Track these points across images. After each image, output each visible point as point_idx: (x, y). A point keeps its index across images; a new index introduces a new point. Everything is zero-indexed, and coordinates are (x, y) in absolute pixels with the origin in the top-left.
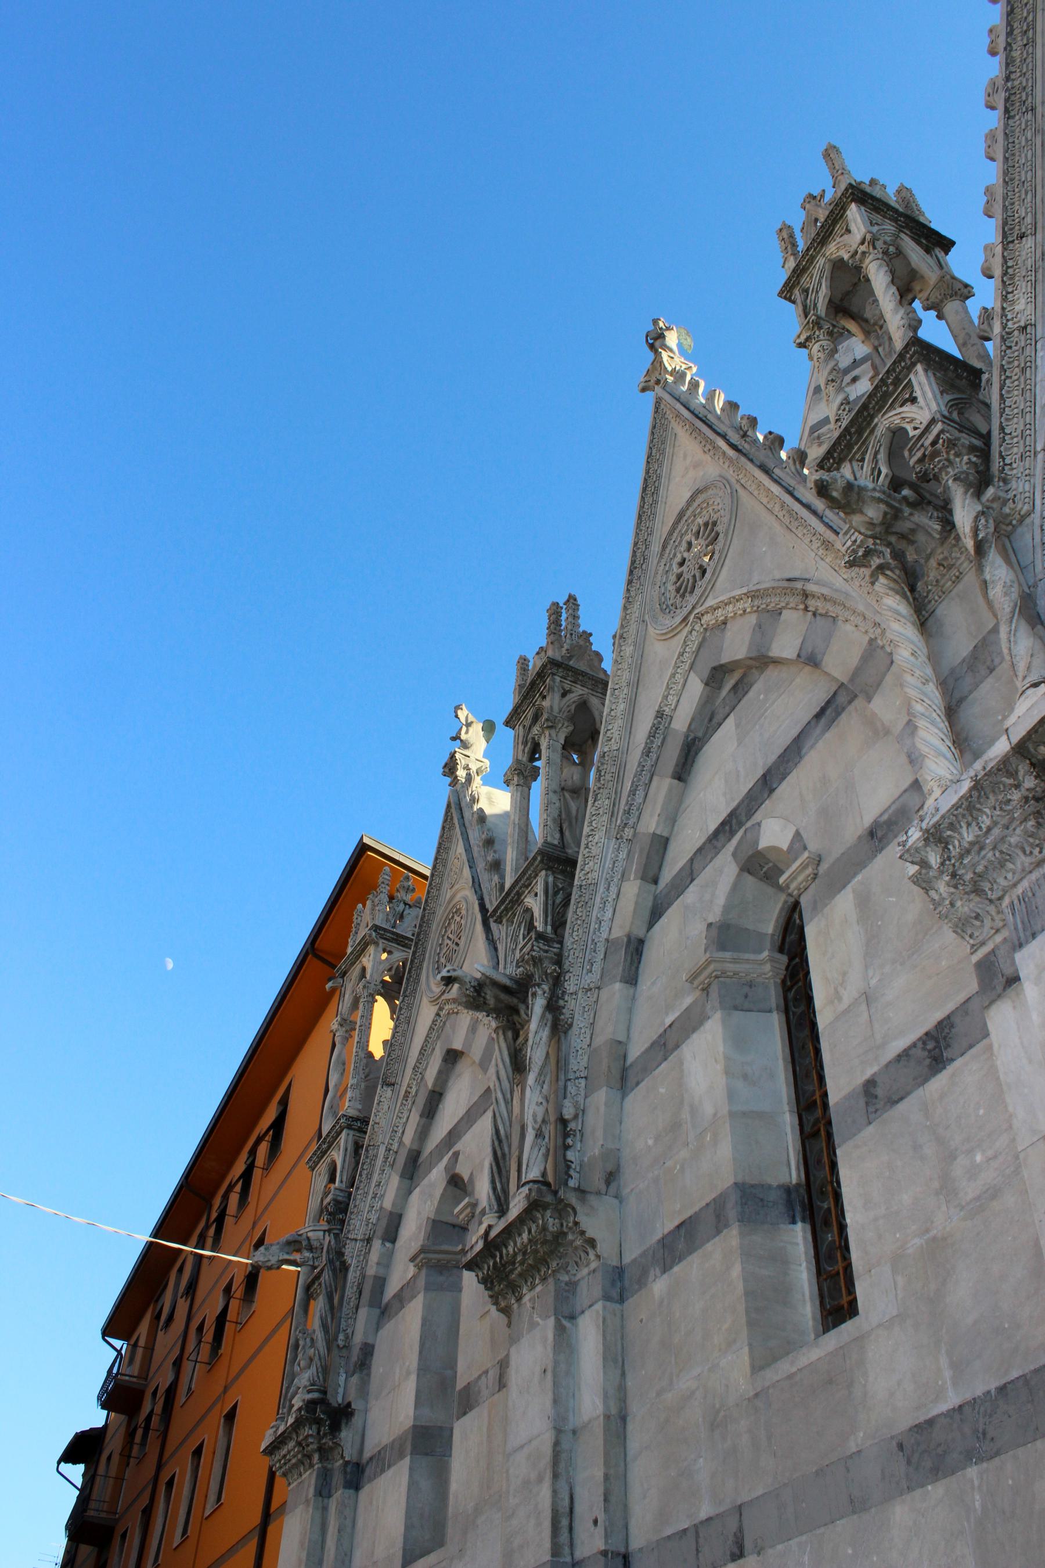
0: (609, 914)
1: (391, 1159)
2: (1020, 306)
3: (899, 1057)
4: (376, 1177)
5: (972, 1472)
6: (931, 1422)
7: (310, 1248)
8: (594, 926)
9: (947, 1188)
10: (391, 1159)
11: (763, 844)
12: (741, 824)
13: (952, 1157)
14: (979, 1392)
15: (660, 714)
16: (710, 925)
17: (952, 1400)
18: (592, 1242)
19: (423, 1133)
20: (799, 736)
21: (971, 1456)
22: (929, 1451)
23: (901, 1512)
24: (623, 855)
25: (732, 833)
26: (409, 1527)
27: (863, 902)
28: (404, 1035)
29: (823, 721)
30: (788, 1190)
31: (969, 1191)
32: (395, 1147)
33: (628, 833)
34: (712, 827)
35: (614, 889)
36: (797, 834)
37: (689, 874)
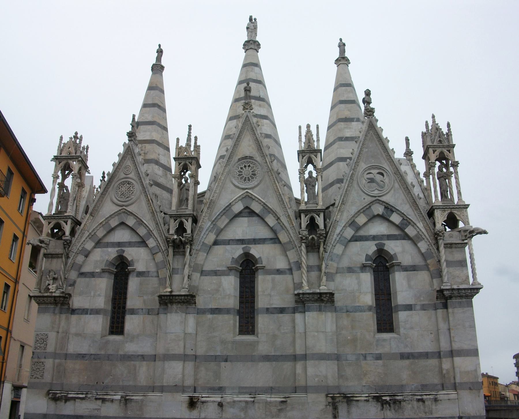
0: (205, 237)
1: (90, 236)
2: (338, 217)
3: (274, 308)
4: (84, 239)
5: (274, 363)
6: (269, 355)
7: (46, 244)
8: (201, 237)
10: (90, 236)
11: (251, 252)
12: (245, 244)
13: (281, 326)
14: (278, 354)
15: (230, 204)
16: (233, 258)
17: (273, 354)
18: (195, 303)
19: (105, 236)
20: (265, 239)
21: (274, 361)
22: (267, 358)
23: (261, 364)
24: (211, 226)
25: (243, 244)
26: (102, 330)
27: (273, 280)
28: (100, 204)
29: (271, 241)
30: (237, 310)
31: (283, 331)
32: (93, 234)
33: (214, 223)
34: (237, 238)
35: (207, 233)
36: (260, 258)
37: (228, 242)
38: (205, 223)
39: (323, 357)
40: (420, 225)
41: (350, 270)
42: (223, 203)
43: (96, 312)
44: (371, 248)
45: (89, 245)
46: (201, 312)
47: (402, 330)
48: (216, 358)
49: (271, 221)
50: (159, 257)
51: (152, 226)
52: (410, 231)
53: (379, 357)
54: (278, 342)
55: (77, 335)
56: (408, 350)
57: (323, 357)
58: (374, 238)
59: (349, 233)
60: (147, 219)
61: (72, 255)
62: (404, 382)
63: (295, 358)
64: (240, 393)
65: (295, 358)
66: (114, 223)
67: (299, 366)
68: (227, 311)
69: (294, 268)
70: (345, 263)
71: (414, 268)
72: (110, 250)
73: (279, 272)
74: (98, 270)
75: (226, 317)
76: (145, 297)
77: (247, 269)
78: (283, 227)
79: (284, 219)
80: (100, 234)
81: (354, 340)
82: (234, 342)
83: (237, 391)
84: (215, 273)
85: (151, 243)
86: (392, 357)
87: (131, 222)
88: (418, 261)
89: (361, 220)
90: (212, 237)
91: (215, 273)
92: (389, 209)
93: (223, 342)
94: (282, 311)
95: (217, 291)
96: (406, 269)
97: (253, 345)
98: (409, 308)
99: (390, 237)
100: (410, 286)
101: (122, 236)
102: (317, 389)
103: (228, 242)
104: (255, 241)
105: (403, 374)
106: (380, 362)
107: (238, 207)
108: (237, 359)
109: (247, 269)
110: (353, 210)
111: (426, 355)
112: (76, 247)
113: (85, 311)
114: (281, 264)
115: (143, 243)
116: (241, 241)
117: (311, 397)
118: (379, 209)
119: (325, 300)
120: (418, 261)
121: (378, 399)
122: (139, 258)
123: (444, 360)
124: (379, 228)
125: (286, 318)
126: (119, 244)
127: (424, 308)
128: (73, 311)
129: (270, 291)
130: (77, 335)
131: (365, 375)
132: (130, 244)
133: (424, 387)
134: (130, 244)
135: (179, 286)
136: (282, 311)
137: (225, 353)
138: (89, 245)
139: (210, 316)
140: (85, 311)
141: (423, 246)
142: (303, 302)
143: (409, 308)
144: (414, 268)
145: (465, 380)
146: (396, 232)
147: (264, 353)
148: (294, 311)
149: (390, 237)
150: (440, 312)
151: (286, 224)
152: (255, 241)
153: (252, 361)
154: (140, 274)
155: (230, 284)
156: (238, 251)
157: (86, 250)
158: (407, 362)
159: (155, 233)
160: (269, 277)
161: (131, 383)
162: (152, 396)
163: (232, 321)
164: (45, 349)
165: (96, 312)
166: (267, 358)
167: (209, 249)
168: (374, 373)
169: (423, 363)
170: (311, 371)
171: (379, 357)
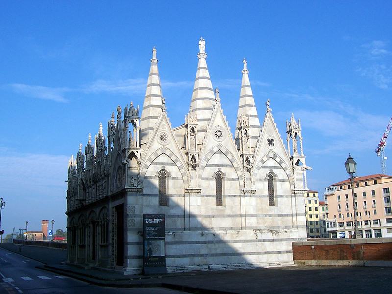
9: (234, 204)
22: (229, 216)
37: (212, 165)
38: (203, 157)
39: (252, 215)
40: (287, 163)
41: (260, 180)
42: (209, 147)
43: (155, 195)
44: (268, 171)
45: (148, 163)
46: (203, 196)
47: (279, 205)
48: (209, 216)
49: (230, 156)
50: (183, 171)
51: (179, 156)
52: (283, 165)
53: (271, 216)
54: (234, 209)
55: (146, 206)
56: (281, 213)
57: (252, 215)
58: (269, 167)
59: (260, 164)
60: (176, 152)
61: (141, 168)
62: (279, 225)
63: (241, 216)
64: (220, 230)
65: (241, 216)
66: (159, 153)
67: (243, 218)
68: (213, 196)
69: (240, 178)
70: (258, 177)
71: (283, 181)
72: (158, 166)
73: (233, 180)
74: (153, 176)
75: (213, 198)
76: (177, 189)
77: (219, 178)
78: (235, 160)
79: (235, 156)
80: (153, 157)
81: (262, 209)
82: (216, 209)
83: (218, 229)
84: (207, 179)
85: (179, 164)
86: (275, 215)
87: (168, 153)
88: (286, 178)
89: (265, 159)
90: (205, 163)
91: (207, 179)
92: (275, 156)
93: (212, 209)
94: (235, 196)
95: (209, 187)
96: (281, 181)
97: (224, 210)
98: (281, 196)
99: (275, 167)
100: (282, 188)
101: (163, 159)
102: (250, 228)
103: (212, 165)
104: (223, 166)
105: (279, 222)
106: (271, 217)
107: (216, 150)
108: (218, 216)
109: (219, 178)
110: (262, 155)
111: (287, 215)
112: (142, 165)
113: (149, 195)
114: (235, 177)
115: (174, 163)
116: (217, 165)
117: (248, 231)
118: (272, 155)
119: (253, 192)
120: (286, 178)
121: (271, 231)
122: (173, 170)
123: (293, 217)
124: (271, 163)
125: (237, 199)
126: (162, 164)
127: (287, 197)
128: (144, 195)
129: (228, 187)
130: (146, 206)
131: (266, 222)
132: (168, 164)
133: (286, 227)
134: (168, 164)
135: (193, 185)
136: (235, 196)
137: (213, 214)
138: (148, 163)
139: (206, 198)
140: (149, 195)
141: (288, 172)
142: (244, 193)
143: (281, 196)
144: (283, 181)
145: (301, 225)
146: (278, 165)
147: (229, 214)
148: (240, 196)
149: (275, 167)
150: (293, 199)
151: (236, 159)
152: (223, 166)
153: (224, 217)
154: (174, 178)
155: (213, 183)
156: (216, 169)
157: (147, 166)
158: (280, 218)
159: (180, 159)
160: (229, 182)
161: (174, 227)
162: (186, 232)
163: (214, 200)
164: (134, 213)
165: (155, 195)
166: (229, 216)
167: (203, 168)
168: (269, 221)
169: (286, 218)
170: (247, 221)
171: (271, 216)
